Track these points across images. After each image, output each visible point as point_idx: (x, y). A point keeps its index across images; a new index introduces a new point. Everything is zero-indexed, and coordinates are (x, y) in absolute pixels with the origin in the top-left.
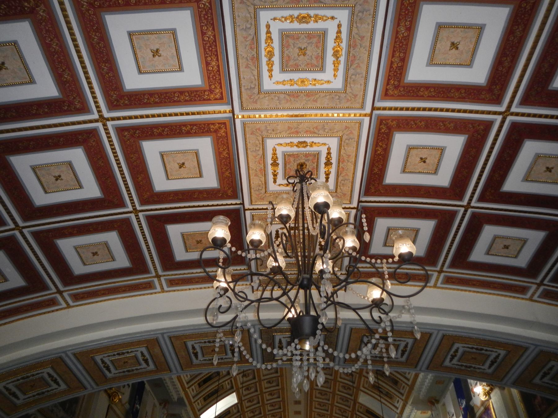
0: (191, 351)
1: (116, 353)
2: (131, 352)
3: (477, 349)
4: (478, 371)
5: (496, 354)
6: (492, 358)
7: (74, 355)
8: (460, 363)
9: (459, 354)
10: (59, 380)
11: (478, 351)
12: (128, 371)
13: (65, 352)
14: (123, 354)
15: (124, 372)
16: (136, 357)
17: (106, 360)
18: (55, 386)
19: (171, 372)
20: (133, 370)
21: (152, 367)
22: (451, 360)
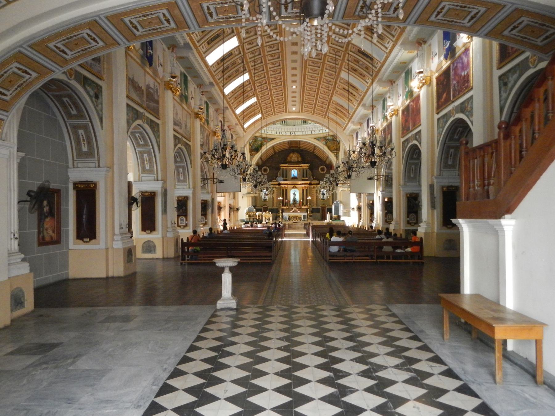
0: (206, 11)
1: (141, 15)
2: (155, 13)
3: (461, 6)
4: (458, 24)
5: (477, 11)
6: (472, 14)
7: (106, 18)
8: (444, 19)
9: (444, 11)
10: (97, 39)
11: (461, 8)
12: (153, 29)
13: (98, 16)
14: (148, 15)
15: (150, 30)
16: (158, 18)
17: (134, 21)
18: (94, 43)
19: (190, 29)
20: (157, 29)
21: (173, 25)
22: (437, 16)
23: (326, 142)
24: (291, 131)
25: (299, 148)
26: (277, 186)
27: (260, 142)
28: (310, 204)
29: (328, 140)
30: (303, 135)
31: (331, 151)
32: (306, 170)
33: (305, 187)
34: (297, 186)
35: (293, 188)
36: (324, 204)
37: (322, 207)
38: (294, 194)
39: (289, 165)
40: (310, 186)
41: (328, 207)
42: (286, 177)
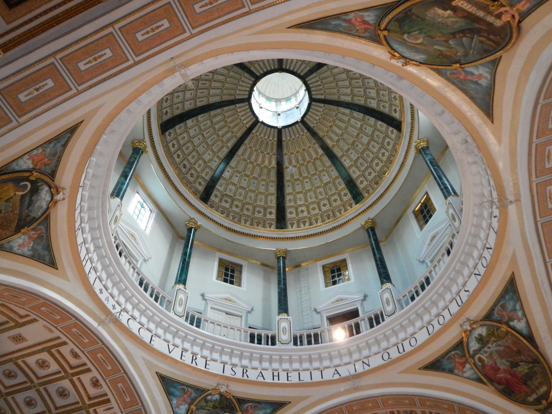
29: (35, 191)
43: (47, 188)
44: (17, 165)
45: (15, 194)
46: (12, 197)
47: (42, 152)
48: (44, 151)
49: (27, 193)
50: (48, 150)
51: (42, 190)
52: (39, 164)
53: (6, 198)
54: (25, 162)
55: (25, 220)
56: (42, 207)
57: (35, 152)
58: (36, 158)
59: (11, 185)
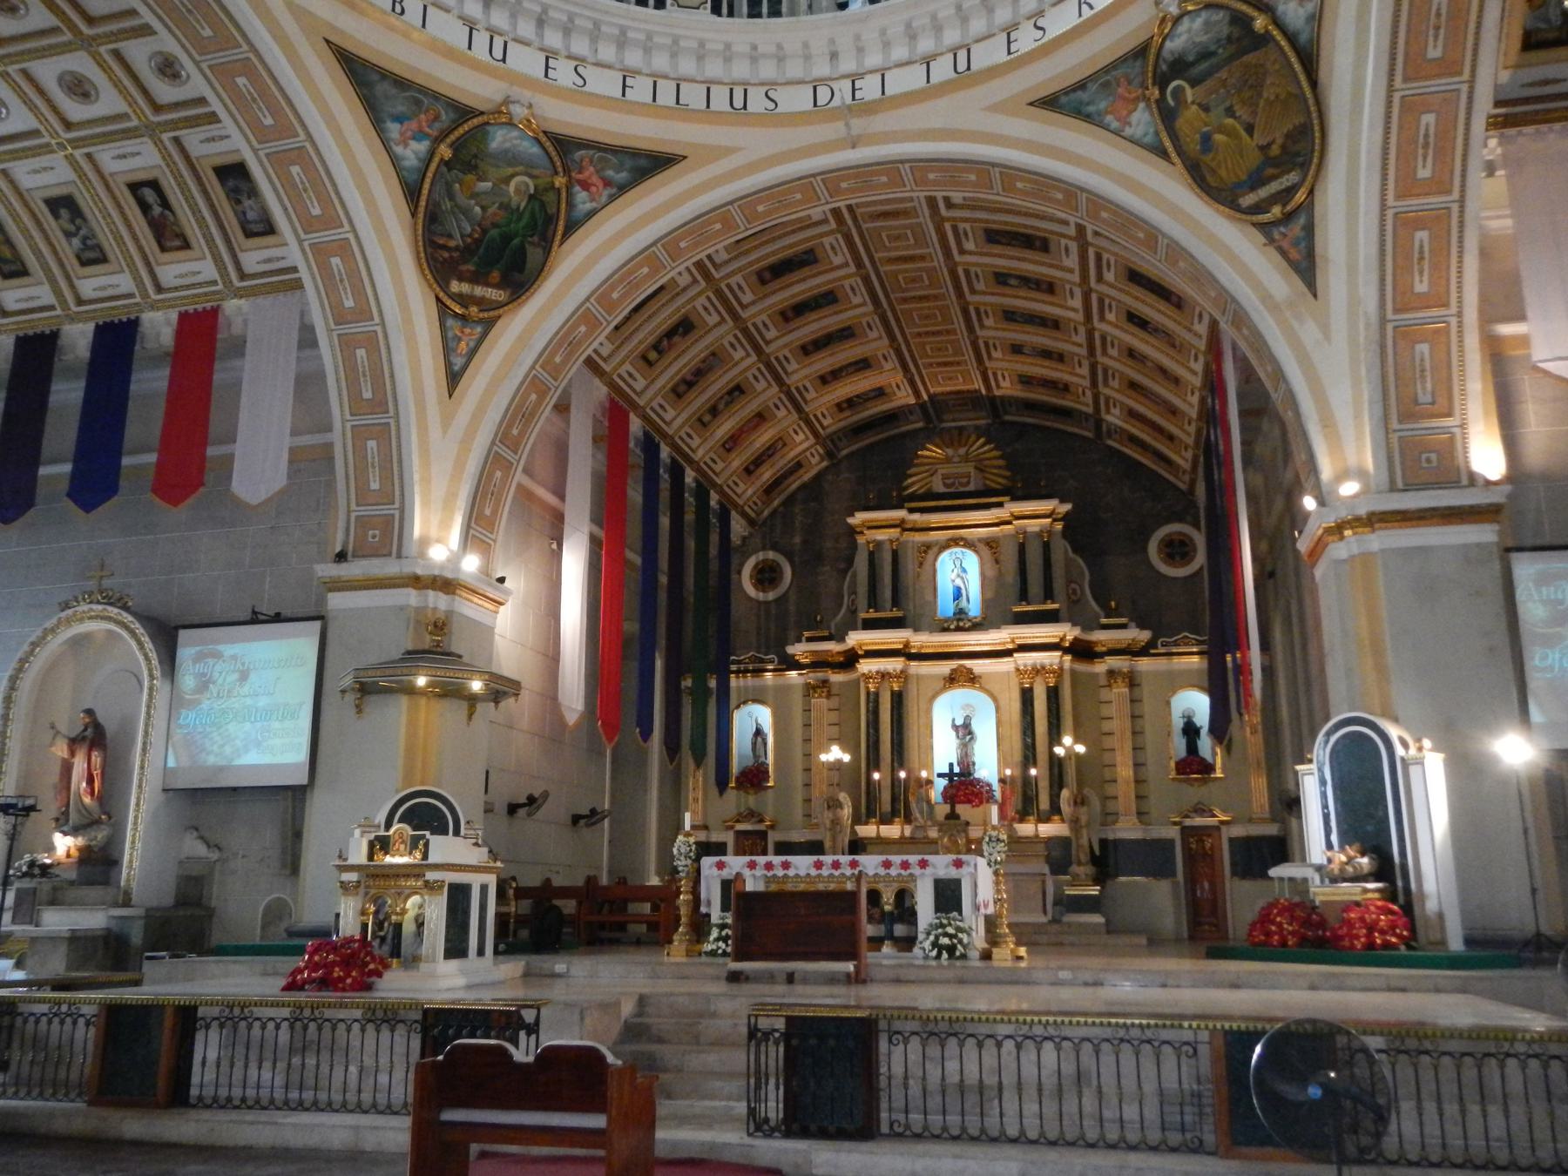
23: (1161, 102)
24: (822, 69)
25: (995, 406)
26: (837, 678)
27: (518, 187)
28: (1080, 801)
29: (1179, 66)
30: (932, 92)
31: (1222, 194)
32: (1046, 547)
33: (1038, 671)
34: (978, 666)
35: (952, 680)
36: (1200, 810)
37: (1187, 832)
38: (965, 731)
39: (916, 517)
40: (1082, 667)
41: (1238, 831)
42: (896, 602)
43: (1169, 45)
44: (1145, 135)
45: (1193, 103)
46: (1200, 105)
47: (1111, 113)
48: (1107, 113)
49: (1185, 80)
50: (1103, 105)
51: (1172, 53)
52: (1134, 95)
53: (1203, 115)
54: (1138, 125)
55: (1238, 39)
56: (1207, 23)
57: (1115, 125)
58: (1124, 113)
59: (1181, 123)
